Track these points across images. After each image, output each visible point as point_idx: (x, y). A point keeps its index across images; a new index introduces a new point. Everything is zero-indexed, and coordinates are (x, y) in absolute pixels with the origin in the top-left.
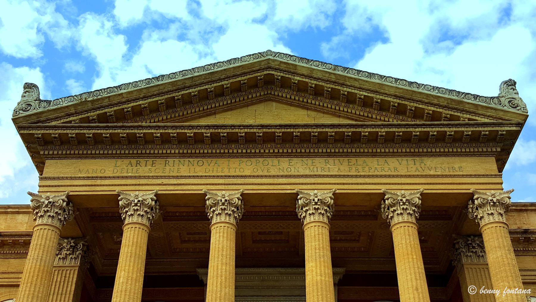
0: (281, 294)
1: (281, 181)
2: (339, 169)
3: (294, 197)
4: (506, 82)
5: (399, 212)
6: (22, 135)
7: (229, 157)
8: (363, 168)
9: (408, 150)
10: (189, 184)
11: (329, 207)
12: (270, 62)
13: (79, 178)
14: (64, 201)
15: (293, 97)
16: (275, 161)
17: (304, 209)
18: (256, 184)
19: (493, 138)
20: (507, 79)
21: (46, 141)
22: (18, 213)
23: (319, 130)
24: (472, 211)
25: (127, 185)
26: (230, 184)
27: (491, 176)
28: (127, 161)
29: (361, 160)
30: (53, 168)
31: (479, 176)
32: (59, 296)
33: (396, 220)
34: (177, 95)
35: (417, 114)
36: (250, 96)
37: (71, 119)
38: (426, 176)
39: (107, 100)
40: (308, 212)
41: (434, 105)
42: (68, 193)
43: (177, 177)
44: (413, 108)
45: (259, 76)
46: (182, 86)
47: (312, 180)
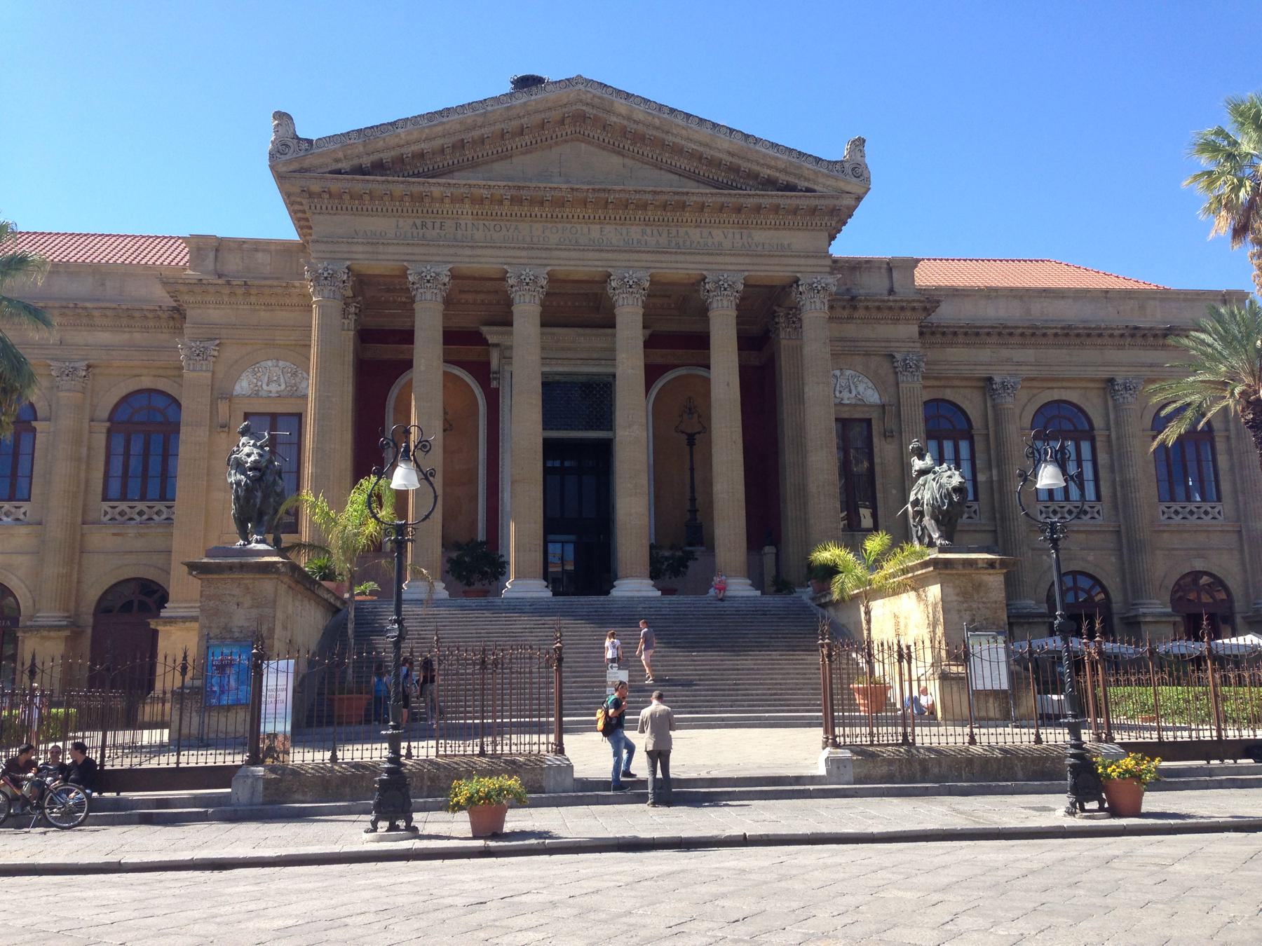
1: (591, 255)
22: (256, 250)
28: (410, 221)
29: (682, 231)
34: (467, 137)
37: (340, 165)
47: (627, 256)
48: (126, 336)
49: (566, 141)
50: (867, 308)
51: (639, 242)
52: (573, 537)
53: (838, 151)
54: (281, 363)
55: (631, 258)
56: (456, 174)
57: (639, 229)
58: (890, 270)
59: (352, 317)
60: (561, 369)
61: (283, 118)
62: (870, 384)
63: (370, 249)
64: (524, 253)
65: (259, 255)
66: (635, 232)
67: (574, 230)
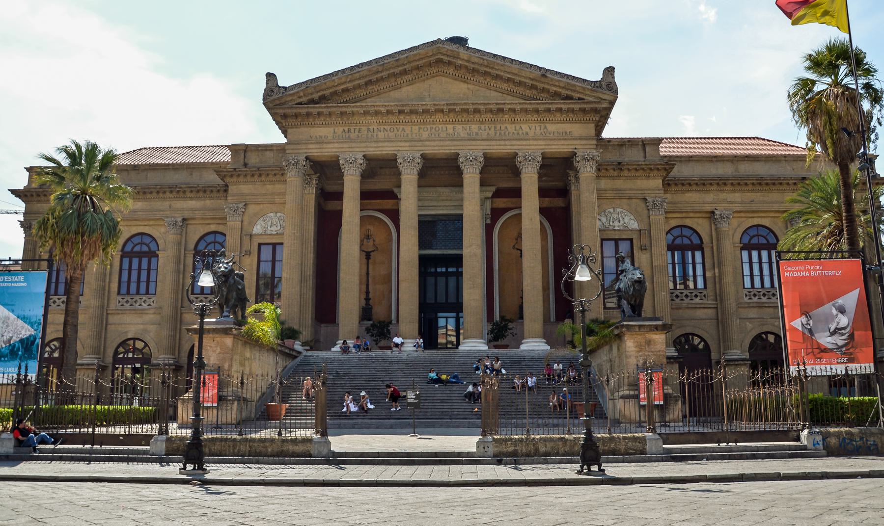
1: (448, 143)
4: (606, 69)
16: (444, 127)
19: (596, 111)
21: (285, 116)
22: (266, 150)
28: (341, 129)
34: (374, 78)
37: (301, 100)
41: (555, 86)
48: (203, 202)
50: (629, 169)
51: (477, 134)
52: (454, 315)
53: (597, 76)
54: (279, 214)
55: (471, 143)
56: (369, 100)
58: (644, 146)
59: (314, 186)
60: (441, 212)
61: (271, 76)
62: (632, 217)
63: (318, 146)
64: (407, 144)
65: (268, 153)
66: (474, 127)
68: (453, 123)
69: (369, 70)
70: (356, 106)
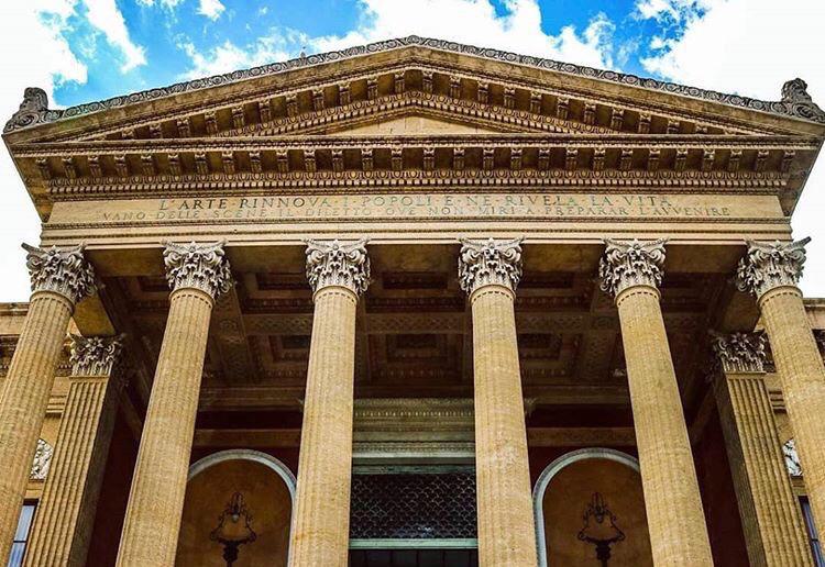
0: (434, 438)
2: (529, 210)
3: (455, 251)
4: (791, 83)
5: (630, 271)
6: (17, 161)
7: (347, 193)
8: (570, 209)
9: (642, 182)
10: (279, 232)
11: (513, 265)
12: (416, 51)
13: (104, 226)
14: (77, 258)
15: (452, 108)
17: (472, 268)
18: (390, 231)
20: (794, 79)
21: (51, 171)
23: (496, 145)
24: (745, 274)
25: (178, 234)
26: (346, 232)
27: (774, 221)
28: (179, 201)
30: (62, 212)
31: (754, 221)
32: (72, 420)
33: (624, 284)
34: (264, 100)
35: (656, 126)
36: (382, 107)
38: (671, 220)
39: (150, 107)
40: (478, 273)
41: (679, 112)
42: (84, 247)
43: (260, 222)
44: (649, 119)
45: (397, 73)
46: (272, 87)
49: (400, 116)
57: (501, 197)
67: (407, 201)
68: (446, 189)
69: (256, 83)
70: (218, 144)
